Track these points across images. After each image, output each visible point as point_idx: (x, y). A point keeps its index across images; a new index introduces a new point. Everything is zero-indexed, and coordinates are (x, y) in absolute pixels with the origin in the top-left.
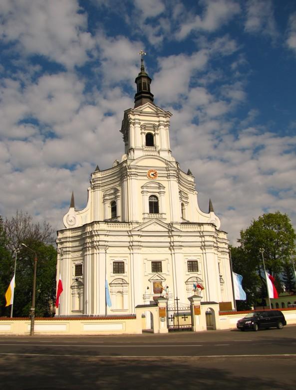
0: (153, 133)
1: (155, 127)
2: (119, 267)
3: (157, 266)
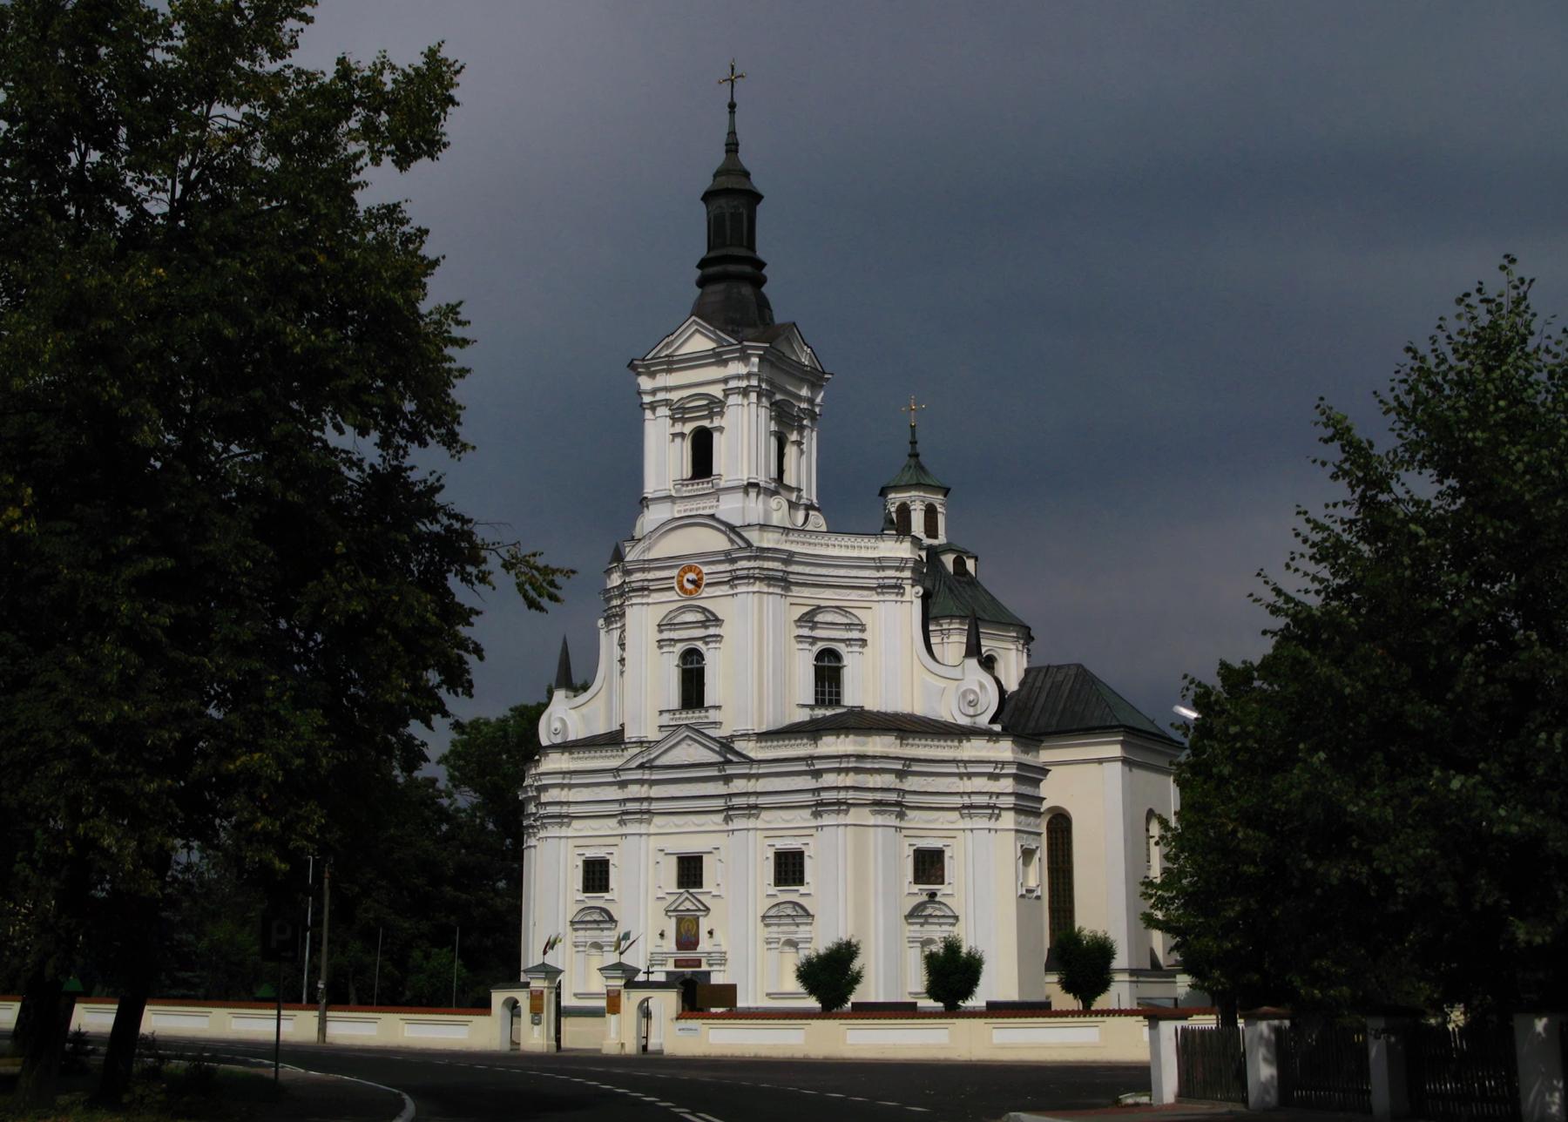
0: (706, 423)
1: (715, 406)
2: (596, 875)
3: (690, 870)
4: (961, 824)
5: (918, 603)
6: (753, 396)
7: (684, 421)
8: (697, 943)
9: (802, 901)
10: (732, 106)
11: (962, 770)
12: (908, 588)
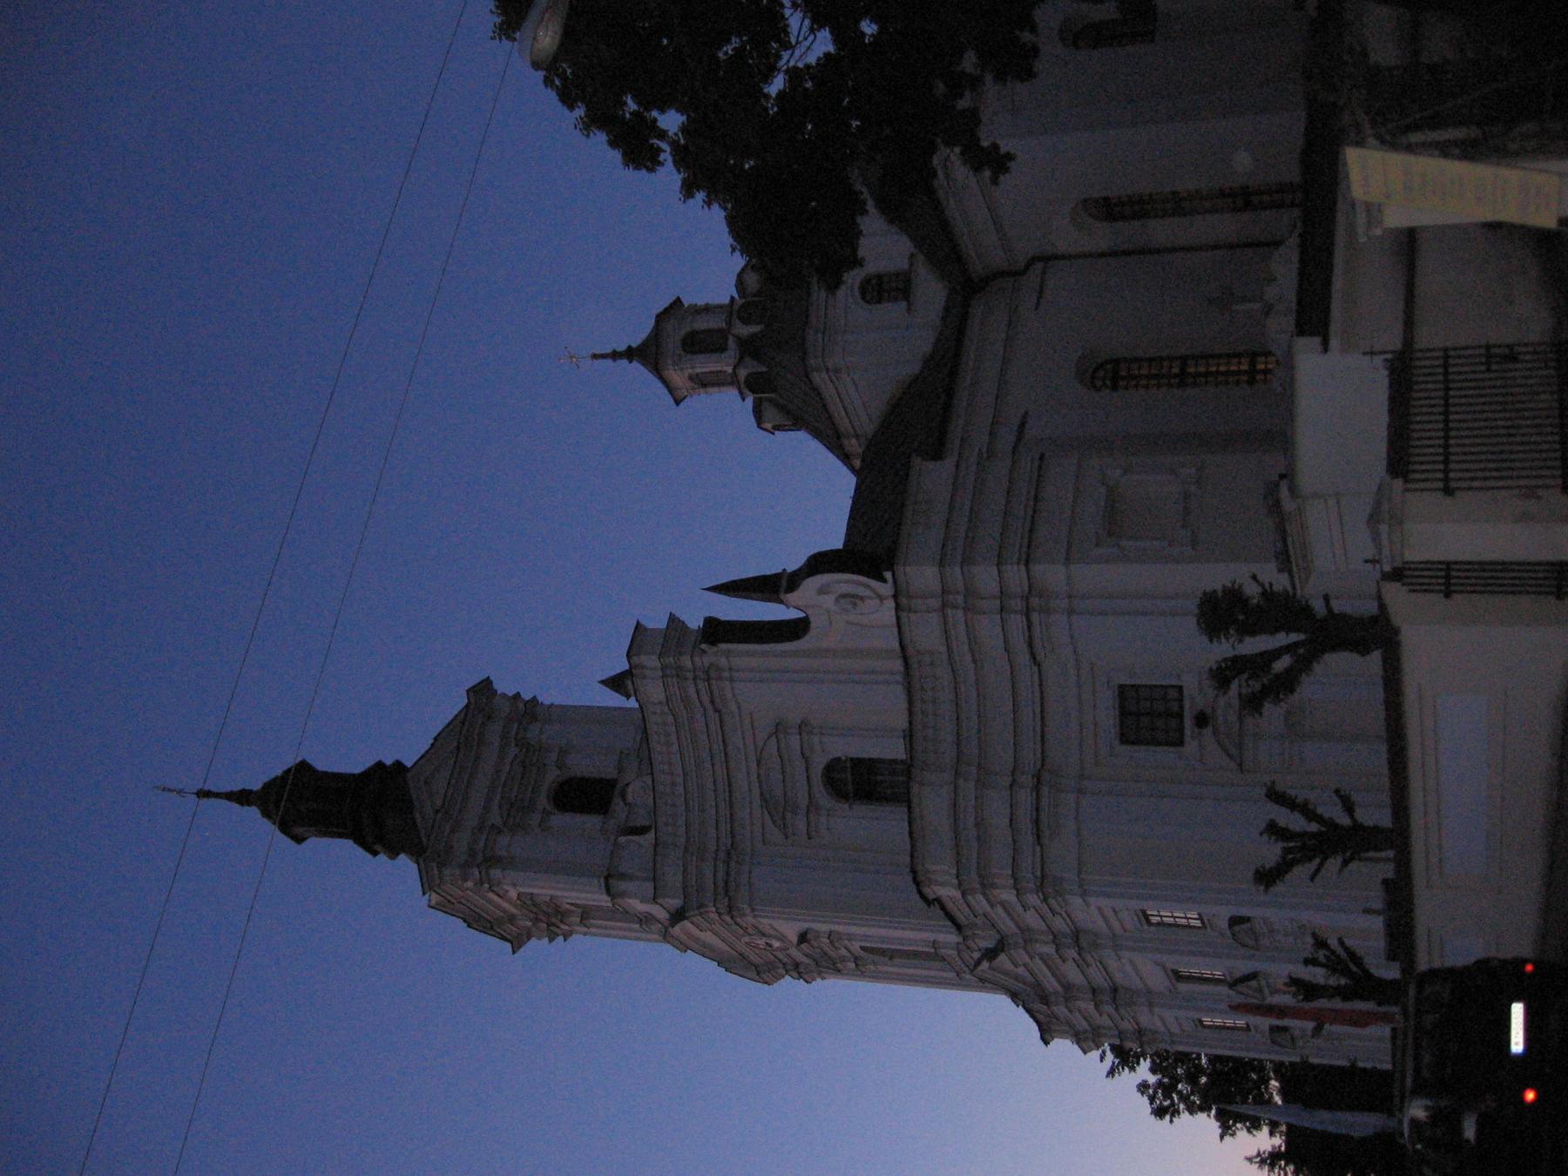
6: (496, 873)
10: (204, 794)
12: (706, 661)
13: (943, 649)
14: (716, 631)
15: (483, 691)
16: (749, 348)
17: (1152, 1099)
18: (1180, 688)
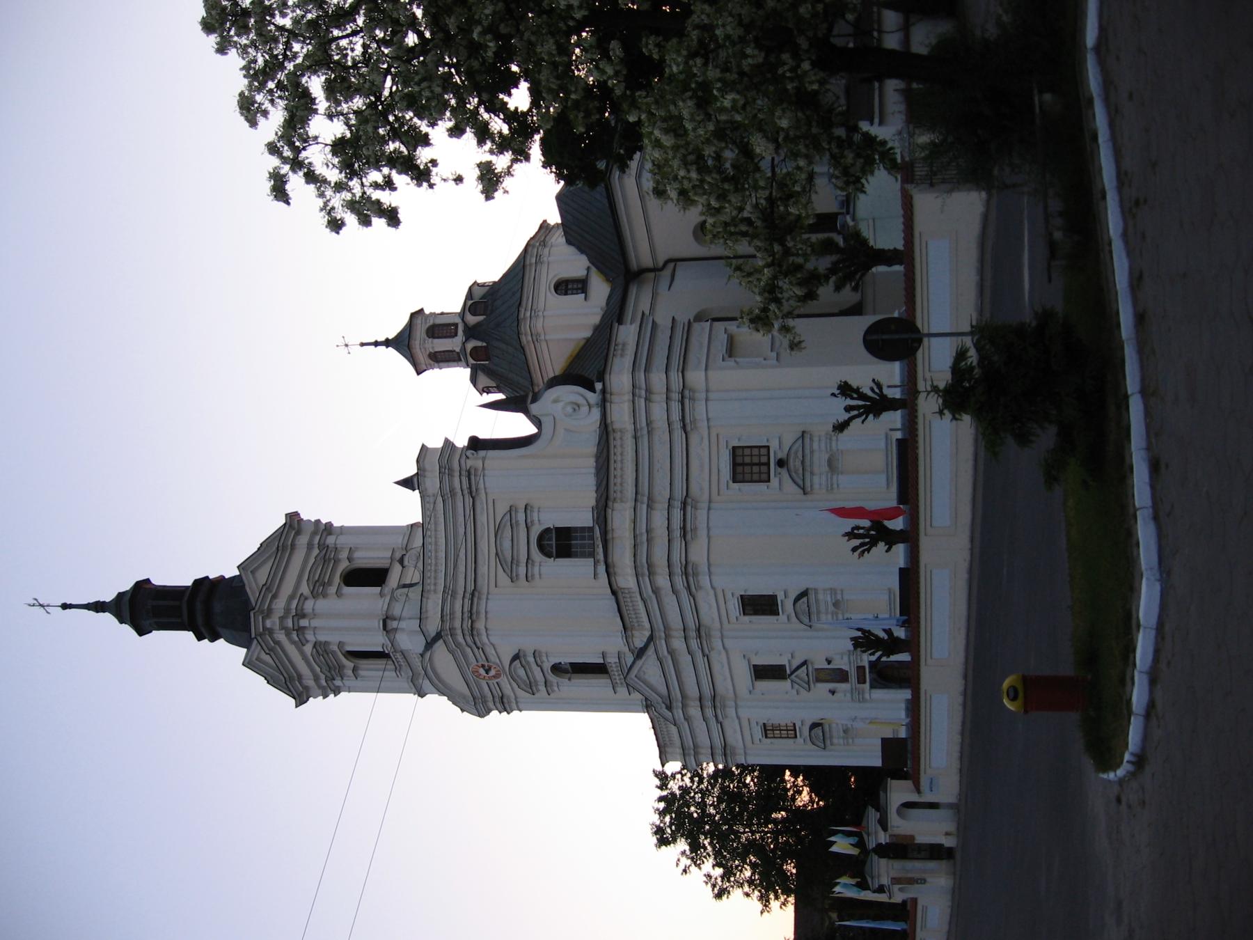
1: (321, 649)
4: (703, 425)
5: (482, 453)
7: (341, 667)
8: (841, 670)
9: (793, 596)
10: (65, 606)
11: (645, 432)
12: (470, 463)
13: (630, 427)
14: (476, 444)
15: (293, 518)
16: (471, 332)
17: (714, 886)
18: (768, 447)
